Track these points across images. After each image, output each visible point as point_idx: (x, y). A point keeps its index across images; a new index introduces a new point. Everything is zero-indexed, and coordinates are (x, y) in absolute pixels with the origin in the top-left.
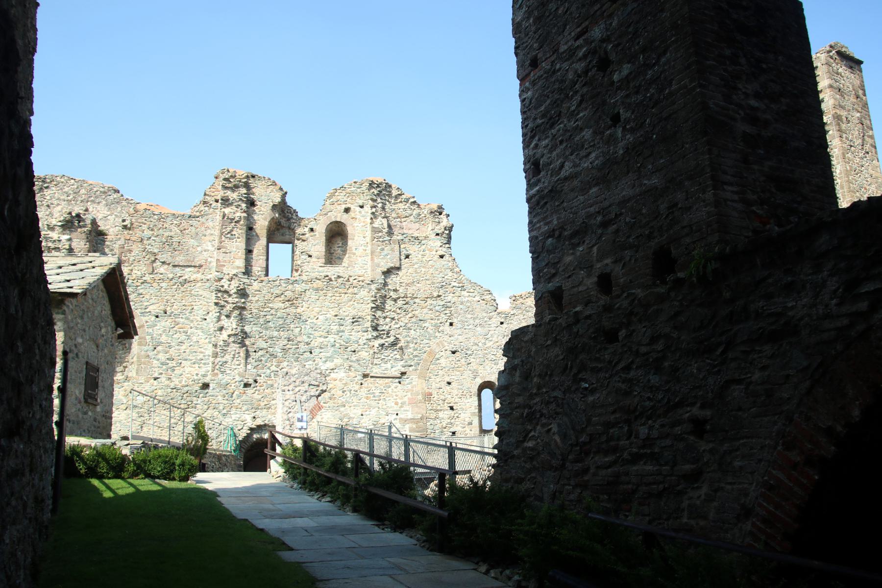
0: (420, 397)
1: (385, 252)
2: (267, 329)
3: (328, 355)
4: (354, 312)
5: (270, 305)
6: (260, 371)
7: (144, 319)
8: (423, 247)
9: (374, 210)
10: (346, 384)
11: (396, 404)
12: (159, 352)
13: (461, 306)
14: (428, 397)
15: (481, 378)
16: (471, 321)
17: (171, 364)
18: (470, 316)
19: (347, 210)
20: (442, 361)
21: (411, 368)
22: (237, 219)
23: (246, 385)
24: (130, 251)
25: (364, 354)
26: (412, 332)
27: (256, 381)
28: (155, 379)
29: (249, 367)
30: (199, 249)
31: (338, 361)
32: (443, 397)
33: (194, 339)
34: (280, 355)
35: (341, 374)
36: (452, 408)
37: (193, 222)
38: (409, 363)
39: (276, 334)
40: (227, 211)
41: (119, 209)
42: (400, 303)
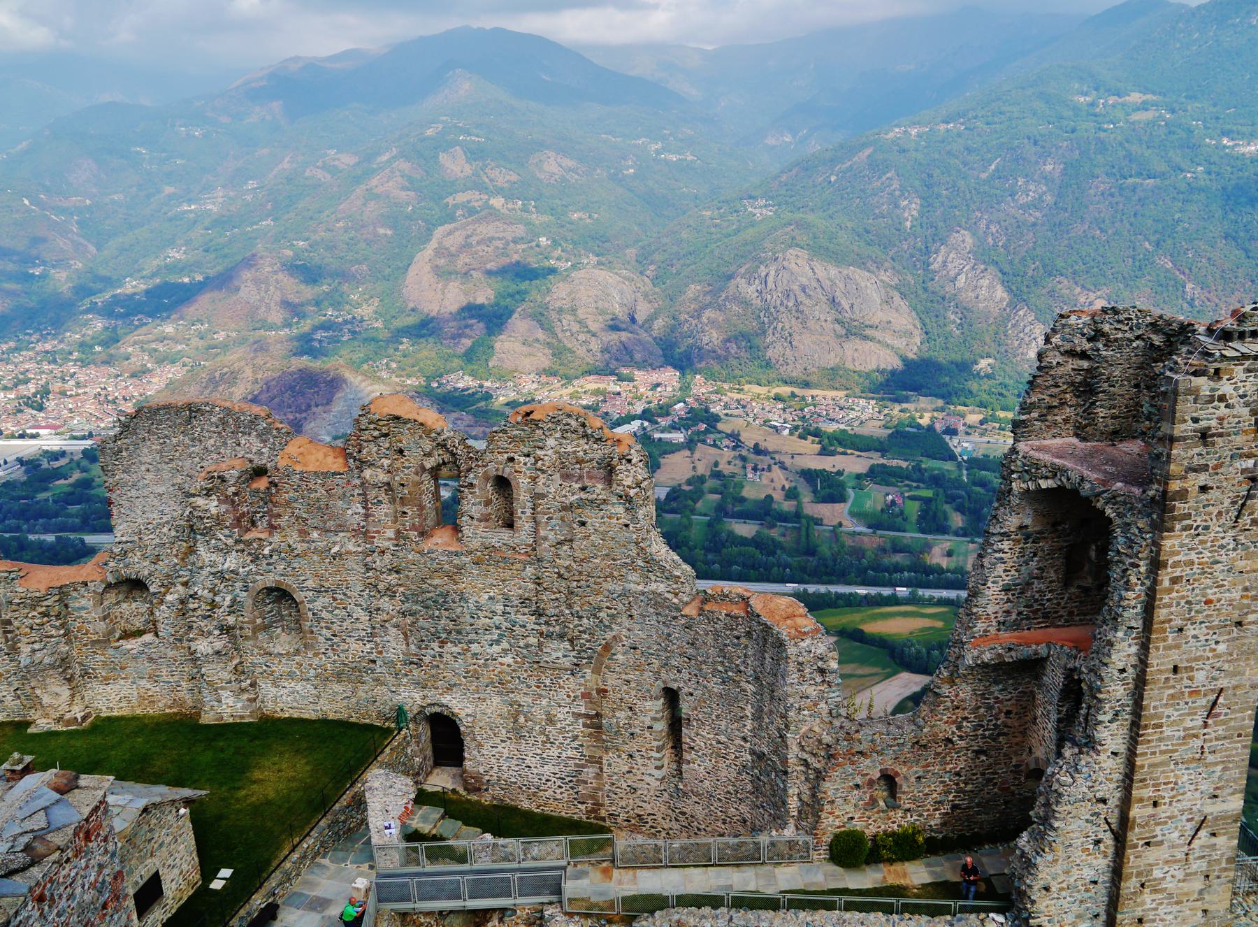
1: (553, 522)
3: (495, 637)
4: (521, 592)
7: (303, 594)
11: (569, 696)
15: (664, 682)
17: (336, 640)
19: (511, 460)
24: (279, 516)
25: (533, 640)
26: (585, 620)
30: (349, 512)
31: (505, 645)
33: (355, 616)
34: (444, 636)
37: (338, 480)
38: (583, 654)
39: (437, 613)
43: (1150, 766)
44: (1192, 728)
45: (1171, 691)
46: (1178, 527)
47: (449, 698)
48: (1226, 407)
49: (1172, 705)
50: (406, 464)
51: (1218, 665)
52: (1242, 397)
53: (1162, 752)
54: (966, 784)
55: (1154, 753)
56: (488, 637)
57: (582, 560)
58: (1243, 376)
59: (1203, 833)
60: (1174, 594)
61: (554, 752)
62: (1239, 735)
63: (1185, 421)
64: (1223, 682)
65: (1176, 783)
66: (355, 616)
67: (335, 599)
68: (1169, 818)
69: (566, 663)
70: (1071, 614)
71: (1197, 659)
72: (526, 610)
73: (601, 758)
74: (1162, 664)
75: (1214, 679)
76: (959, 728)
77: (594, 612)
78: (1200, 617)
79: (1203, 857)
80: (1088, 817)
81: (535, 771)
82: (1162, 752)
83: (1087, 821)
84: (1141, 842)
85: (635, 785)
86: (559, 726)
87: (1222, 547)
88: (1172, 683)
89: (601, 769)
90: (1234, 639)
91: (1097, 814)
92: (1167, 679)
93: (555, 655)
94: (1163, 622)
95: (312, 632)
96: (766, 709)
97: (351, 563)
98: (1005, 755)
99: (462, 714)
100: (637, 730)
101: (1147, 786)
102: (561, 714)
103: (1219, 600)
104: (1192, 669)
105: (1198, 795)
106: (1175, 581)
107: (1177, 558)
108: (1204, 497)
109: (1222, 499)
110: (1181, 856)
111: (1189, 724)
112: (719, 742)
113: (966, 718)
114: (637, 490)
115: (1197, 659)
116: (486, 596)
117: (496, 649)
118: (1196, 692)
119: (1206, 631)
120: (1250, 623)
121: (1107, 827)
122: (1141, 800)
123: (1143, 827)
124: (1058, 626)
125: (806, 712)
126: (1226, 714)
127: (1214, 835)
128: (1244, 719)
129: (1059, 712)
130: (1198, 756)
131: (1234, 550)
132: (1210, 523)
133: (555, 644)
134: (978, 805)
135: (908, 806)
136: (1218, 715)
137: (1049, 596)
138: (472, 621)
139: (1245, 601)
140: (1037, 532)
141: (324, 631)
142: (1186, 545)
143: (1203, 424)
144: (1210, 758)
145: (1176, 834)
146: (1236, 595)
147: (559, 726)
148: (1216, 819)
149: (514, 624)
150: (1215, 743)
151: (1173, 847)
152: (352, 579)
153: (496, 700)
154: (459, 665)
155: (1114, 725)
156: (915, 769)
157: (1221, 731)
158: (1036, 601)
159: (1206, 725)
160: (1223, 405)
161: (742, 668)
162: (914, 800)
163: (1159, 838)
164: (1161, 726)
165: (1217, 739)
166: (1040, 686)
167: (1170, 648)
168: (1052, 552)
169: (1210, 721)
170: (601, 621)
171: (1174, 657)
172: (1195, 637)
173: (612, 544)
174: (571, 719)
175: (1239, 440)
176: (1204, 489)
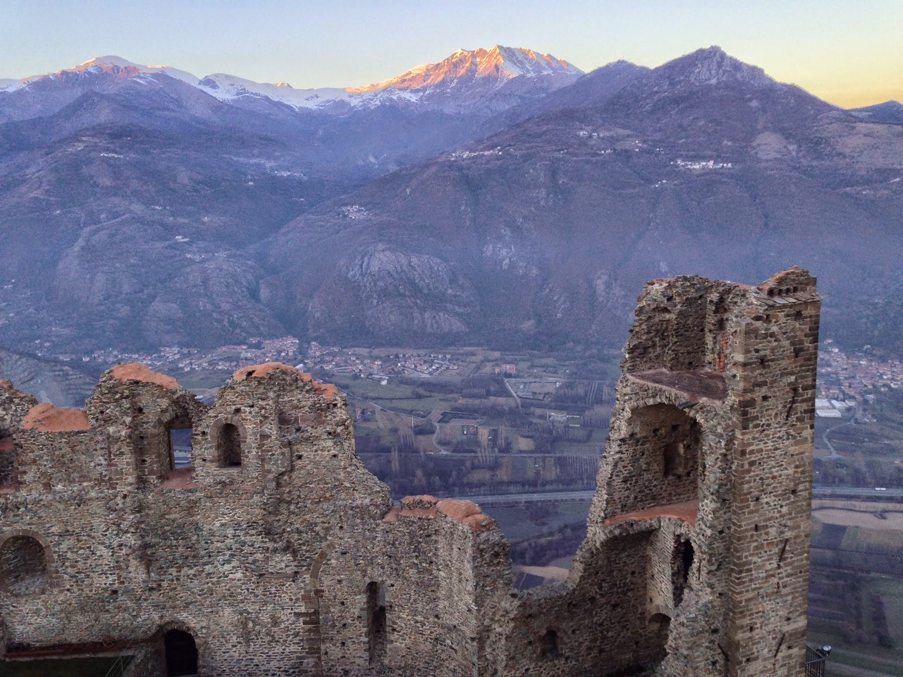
0: (312, 594)
2: (165, 539)
3: (227, 557)
4: (249, 517)
5: (167, 517)
6: (163, 577)
7: (49, 539)
8: (315, 448)
9: (263, 411)
10: (243, 584)
11: (291, 600)
12: (67, 567)
13: (350, 512)
14: (319, 593)
16: (361, 526)
18: (359, 521)
20: (333, 561)
21: (304, 568)
22: (122, 439)
23: (151, 589)
24: (25, 473)
25: (259, 556)
27: (160, 585)
28: (68, 590)
29: (152, 574)
32: (333, 594)
33: (98, 553)
35: (239, 575)
36: (343, 603)
40: (111, 430)
41: (14, 408)
42: (292, 507)
43: (746, 601)
44: (771, 570)
45: (755, 544)
46: (751, 426)
47: (185, 615)
48: (775, 341)
49: (757, 554)
50: (145, 420)
51: (783, 522)
52: (785, 333)
53: (753, 590)
54: (608, 632)
55: (747, 591)
56: (221, 558)
57: (300, 487)
58: (784, 320)
59: (783, 647)
60: (752, 474)
61: (279, 649)
62: (801, 572)
63: (750, 352)
64: (788, 534)
65: (763, 612)
66: (98, 553)
67: (79, 541)
68: (760, 638)
69: (289, 571)
70: (670, 495)
71: (769, 519)
72: (254, 532)
73: (319, 648)
74: (748, 524)
75: (782, 533)
76: (600, 588)
77: (311, 526)
78: (770, 489)
79: (784, 665)
80: (707, 644)
81: (262, 668)
82: (753, 590)
83: (707, 647)
84: (744, 659)
85: (347, 668)
86: (283, 626)
87: (779, 438)
88: (755, 538)
89: (319, 658)
90: (794, 502)
91: (712, 642)
92: (752, 536)
93: (279, 566)
94: (746, 494)
95: (57, 572)
96: (455, 590)
97: (95, 507)
98: (633, 606)
99: (198, 627)
100: (349, 621)
101: (744, 616)
102: (286, 617)
103: (780, 476)
104: (767, 527)
105: (778, 618)
106: (752, 464)
107: (751, 448)
108: (766, 403)
109: (777, 405)
110: (770, 666)
111: (769, 567)
112: (417, 622)
113: (604, 580)
114: (342, 427)
115: (769, 519)
116: (218, 524)
117: (227, 567)
118: (772, 543)
119: (773, 498)
120: (801, 491)
121: (720, 651)
122: (742, 627)
123: (745, 647)
124: (662, 505)
125: (488, 588)
126: (791, 558)
127: (790, 648)
128: (802, 560)
129: (672, 569)
130: (775, 590)
131: (788, 439)
132: (771, 422)
133: (278, 557)
134: (617, 647)
135: (567, 654)
136: (786, 559)
137: (655, 483)
138: (206, 546)
139: (796, 475)
140: (645, 437)
141: (69, 570)
142: (757, 438)
143: (762, 353)
144: (784, 591)
145: (766, 650)
146: (791, 471)
147: (283, 626)
148: (791, 635)
149: (243, 544)
150: (786, 579)
151: (765, 660)
152: (96, 522)
153: (228, 611)
154: (195, 585)
155: (719, 573)
156: (571, 624)
157: (789, 569)
158: (646, 487)
159: (779, 567)
160: (773, 339)
161: (434, 559)
162: (572, 649)
163: (756, 654)
164: (750, 570)
165: (787, 576)
166: (654, 550)
167: (750, 512)
168: (654, 451)
169: (781, 564)
170: (317, 534)
171: (756, 518)
172: (767, 503)
173: (324, 471)
174: (293, 618)
175: (784, 363)
176: (765, 398)
